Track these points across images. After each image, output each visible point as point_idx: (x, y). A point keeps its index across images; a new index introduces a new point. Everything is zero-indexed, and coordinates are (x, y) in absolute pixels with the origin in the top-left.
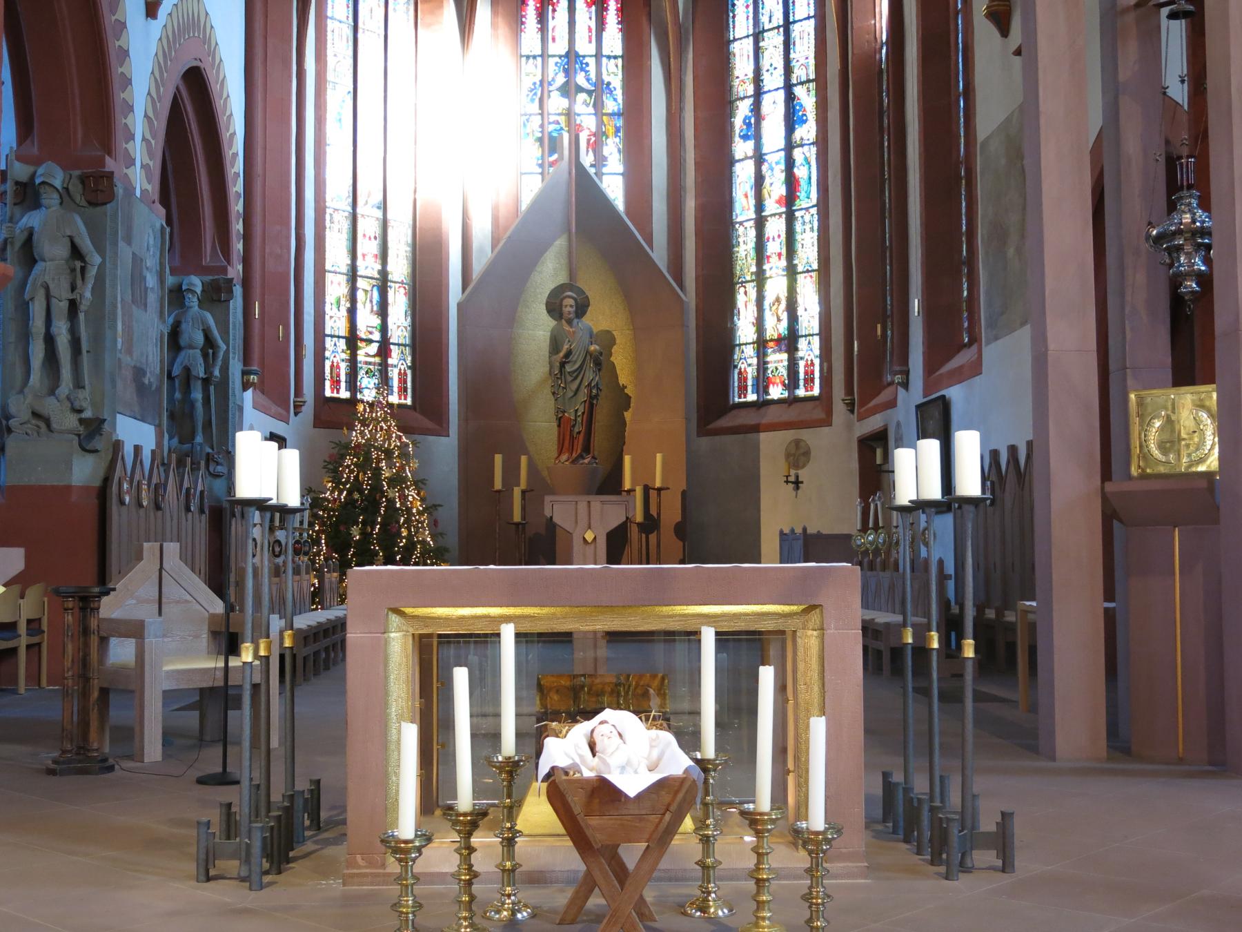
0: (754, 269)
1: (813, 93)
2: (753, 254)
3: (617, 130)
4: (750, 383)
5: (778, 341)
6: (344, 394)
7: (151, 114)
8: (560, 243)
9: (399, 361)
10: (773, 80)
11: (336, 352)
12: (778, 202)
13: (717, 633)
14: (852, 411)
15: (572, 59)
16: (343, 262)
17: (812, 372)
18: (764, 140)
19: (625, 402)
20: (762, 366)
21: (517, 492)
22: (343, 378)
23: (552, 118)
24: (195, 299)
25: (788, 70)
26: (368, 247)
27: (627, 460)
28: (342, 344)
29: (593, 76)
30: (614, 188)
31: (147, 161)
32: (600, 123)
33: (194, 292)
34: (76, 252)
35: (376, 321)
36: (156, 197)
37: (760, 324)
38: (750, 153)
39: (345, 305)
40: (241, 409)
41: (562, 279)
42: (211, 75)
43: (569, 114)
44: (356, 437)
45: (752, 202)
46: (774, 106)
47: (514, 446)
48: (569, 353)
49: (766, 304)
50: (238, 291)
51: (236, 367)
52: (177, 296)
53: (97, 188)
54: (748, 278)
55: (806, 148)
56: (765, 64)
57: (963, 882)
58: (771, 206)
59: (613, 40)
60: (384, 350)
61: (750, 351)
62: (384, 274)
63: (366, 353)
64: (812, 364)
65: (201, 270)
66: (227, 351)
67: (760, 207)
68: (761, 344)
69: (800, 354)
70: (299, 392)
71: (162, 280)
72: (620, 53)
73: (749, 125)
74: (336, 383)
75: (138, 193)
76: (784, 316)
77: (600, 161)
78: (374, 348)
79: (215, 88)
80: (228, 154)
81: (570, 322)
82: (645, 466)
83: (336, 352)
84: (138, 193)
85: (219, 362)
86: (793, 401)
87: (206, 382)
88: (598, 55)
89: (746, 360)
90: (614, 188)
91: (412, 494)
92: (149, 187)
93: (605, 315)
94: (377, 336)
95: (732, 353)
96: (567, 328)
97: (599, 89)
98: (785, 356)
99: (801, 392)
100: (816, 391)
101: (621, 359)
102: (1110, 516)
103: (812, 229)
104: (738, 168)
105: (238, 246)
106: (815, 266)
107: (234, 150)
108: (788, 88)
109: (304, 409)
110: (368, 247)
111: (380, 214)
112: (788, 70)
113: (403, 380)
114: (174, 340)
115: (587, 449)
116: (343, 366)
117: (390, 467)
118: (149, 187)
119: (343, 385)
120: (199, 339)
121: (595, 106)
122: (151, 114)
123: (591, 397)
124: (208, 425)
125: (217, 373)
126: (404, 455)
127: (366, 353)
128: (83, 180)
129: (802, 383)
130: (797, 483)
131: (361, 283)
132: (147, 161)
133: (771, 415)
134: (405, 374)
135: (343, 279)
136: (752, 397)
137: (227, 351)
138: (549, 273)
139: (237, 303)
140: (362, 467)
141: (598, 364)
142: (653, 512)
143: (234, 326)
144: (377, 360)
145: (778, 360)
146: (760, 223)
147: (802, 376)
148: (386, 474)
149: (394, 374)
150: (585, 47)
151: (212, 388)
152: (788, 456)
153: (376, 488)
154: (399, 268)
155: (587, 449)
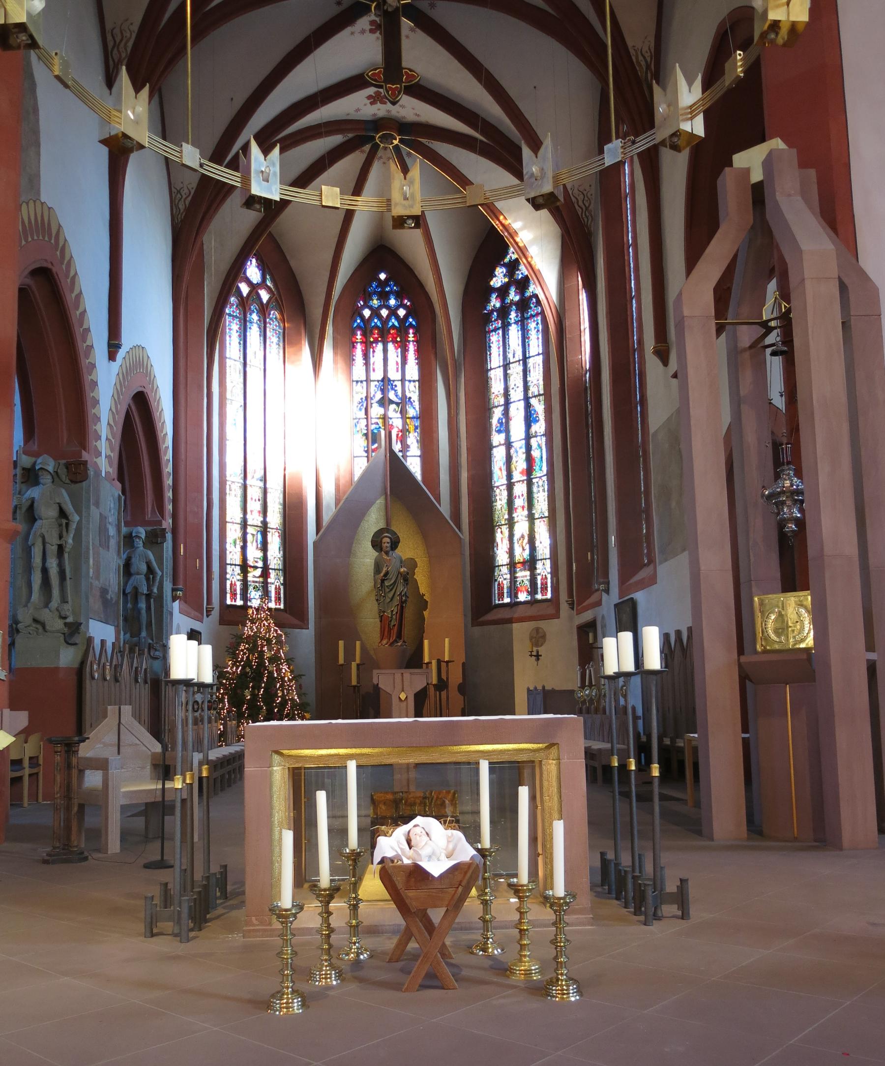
0: (506, 516)
1: (543, 402)
2: (505, 506)
3: (416, 428)
4: (505, 591)
5: (524, 563)
6: (239, 602)
7: (112, 423)
8: (380, 501)
9: (275, 580)
10: (517, 394)
11: (234, 575)
12: (522, 473)
13: (490, 763)
14: (573, 609)
15: (386, 382)
17: (546, 584)
18: (512, 433)
19: (424, 605)
20: (513, 579)
21: (354, 665)
22: (238, 592)
23: (374, 421)
24: (141, 542)
25: (526, 388)
26: (254, 506)
27: (426, 642)
28: (238, 570)
29: (400, 393)
30: (414, 465)
31: (109, 453)
32: (405, 424)
33: (140, 538)
34: (63, 514)
35: (260, 554)
36: (115, 476)
37: (511, 552)
38: (503, 442)
39: (239, 544)
40: (171, 614)
41: (382, 525)
42: (151, 397)
43: (385, 418)
44: (248, 630)
45: (504, 473)
46: (517, 412)
47: (351, 634)
48: (387, 574)
49: (515, 539)
50: (169, 536)
51: (168, 586)
52: (129, 540)
53: (76, 472)
54: (503, 523)
55: (539, 438)
56: (511, 384)
57: (656, 927)
58: (517, 476)
59: (413, 370)
60: (265, 573)
61: (505, 570)
62: (265, 524)
63: (254, 575)
64: (546, 578)
65: (144, 523)
66: (162, 576)
67: (509, 476)
69: (538, 571)
71: (119, 530)
72: (417, 378)
73: (501, 424)
74: (233, 596)
75: (103, 475)
76: (527, 547)
77: (405, 447)
78: (258, 572)
79: (153, 405)
80: (162, 447)
81: (387, 553)
82: (437, 647)
83: (234, 575)
84: (103, 475)
85: (157, 584)
86: (533, 602)
87: (148, 596)
88: (403, 380)
89: (503, 575)
90: (414, 465)
91: (285, 667)
92: (111, 470)
93: (410, 548)
94: (260, 564)
95: (494, 572)
96: (385, 557)
97: (404, 402)
98: (528, 573)
99: (539, 596)
100: (549, 596)
101: (421, 577)
102: (744, 678)
103: (544, 490)
104: (495, 451)
105: (169, 507)
106: (546, 514)
107: (166, 445)
108: (527, 399)
109: (213, 612)
110: (254, 506)
111: (262, 484)
112: (526, 388)
113: (278, 593)
114: (127, 569)
115: (399, 636)
116: (238, 584)
117: (270, 650)
118: (111, 470)
119: (238, 596)
120: (144, 568)
121: (401, 412)
122: (112, 423)
123: (402, 602)
124: (149, 624)
125: (155, 590)
126: (279, 642)
127: (254, 575)
128: (67, 466)
129: (539, 590)
130: (538, 656)
131: (250, 530)
132: (109, 453)
133: (519, 612)
134: (279, 588)
135: (238, 527)
136: (507, 600)
137: (162, 576)
138: (373, 521)
140: (251, 651)
141: (406, 580)
142: (444, 677)
143: (167, 559)
144: (261, 579)
145: (523, 575)
146: (510, 487)
147: (539, 586)
148: (267, 655)
149: (272, 589)
150: (394, 374)
151: (152, 600)
152: (531, 638)
153: (261, 664)
154: (275, 519)
155: (399, 636)
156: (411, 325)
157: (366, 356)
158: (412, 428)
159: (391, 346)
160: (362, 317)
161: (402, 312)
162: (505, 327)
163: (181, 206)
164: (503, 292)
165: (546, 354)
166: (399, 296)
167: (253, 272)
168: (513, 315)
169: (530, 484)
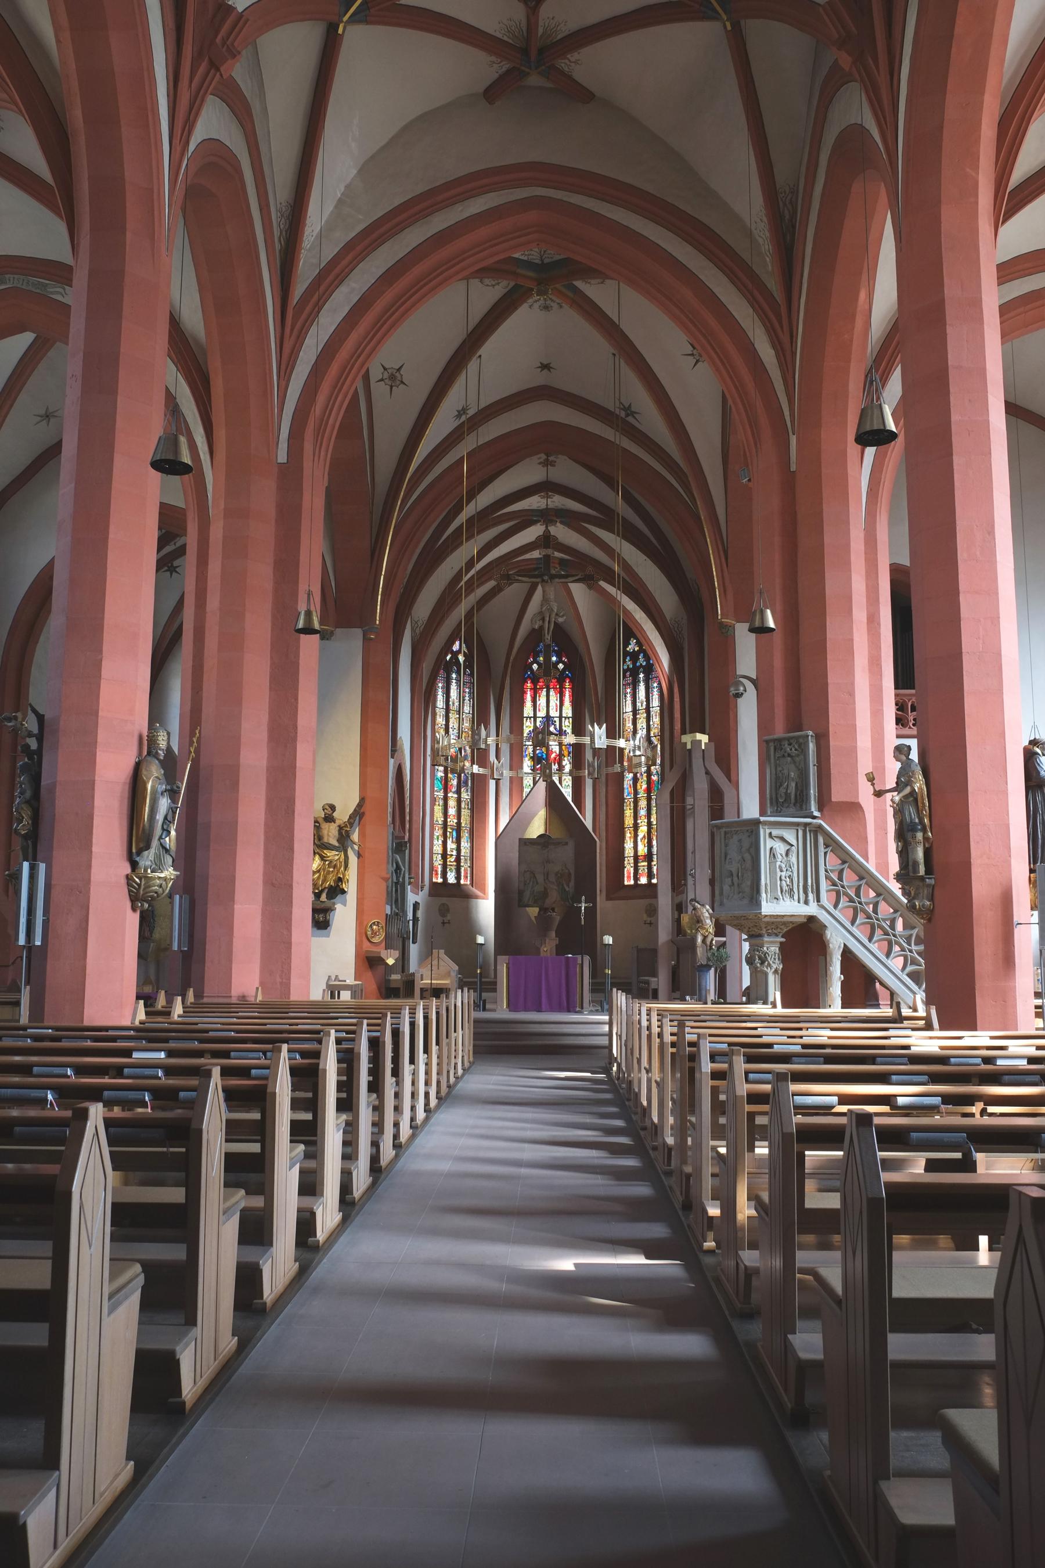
6: (440, 880)
15: (548, 718)
16: (441, 820)
26: (452, 811)
32: (561, 749)
35: (454, 846)
39: (441, 839)
58: (642, 794)
59: (568, 710)
60: (458, 859)
62: (459, 823)
63: (451, 860)
67: (636, 793)
68: (636, 857)
70: (423, 881)
83: (438, 862)
88: (561, 717)
94: (455, 853)
127: (451, 860)
139: (407, 852)
150: (554, 713)
156: (567, 676)
158: (566, 753)
159: (552, 692)
160: (532, 670)
161: (561, 666)
163: (418, 631)
164: (634, 656)
165: (662, 706)
168: (641, 676)
169: (649, 799)
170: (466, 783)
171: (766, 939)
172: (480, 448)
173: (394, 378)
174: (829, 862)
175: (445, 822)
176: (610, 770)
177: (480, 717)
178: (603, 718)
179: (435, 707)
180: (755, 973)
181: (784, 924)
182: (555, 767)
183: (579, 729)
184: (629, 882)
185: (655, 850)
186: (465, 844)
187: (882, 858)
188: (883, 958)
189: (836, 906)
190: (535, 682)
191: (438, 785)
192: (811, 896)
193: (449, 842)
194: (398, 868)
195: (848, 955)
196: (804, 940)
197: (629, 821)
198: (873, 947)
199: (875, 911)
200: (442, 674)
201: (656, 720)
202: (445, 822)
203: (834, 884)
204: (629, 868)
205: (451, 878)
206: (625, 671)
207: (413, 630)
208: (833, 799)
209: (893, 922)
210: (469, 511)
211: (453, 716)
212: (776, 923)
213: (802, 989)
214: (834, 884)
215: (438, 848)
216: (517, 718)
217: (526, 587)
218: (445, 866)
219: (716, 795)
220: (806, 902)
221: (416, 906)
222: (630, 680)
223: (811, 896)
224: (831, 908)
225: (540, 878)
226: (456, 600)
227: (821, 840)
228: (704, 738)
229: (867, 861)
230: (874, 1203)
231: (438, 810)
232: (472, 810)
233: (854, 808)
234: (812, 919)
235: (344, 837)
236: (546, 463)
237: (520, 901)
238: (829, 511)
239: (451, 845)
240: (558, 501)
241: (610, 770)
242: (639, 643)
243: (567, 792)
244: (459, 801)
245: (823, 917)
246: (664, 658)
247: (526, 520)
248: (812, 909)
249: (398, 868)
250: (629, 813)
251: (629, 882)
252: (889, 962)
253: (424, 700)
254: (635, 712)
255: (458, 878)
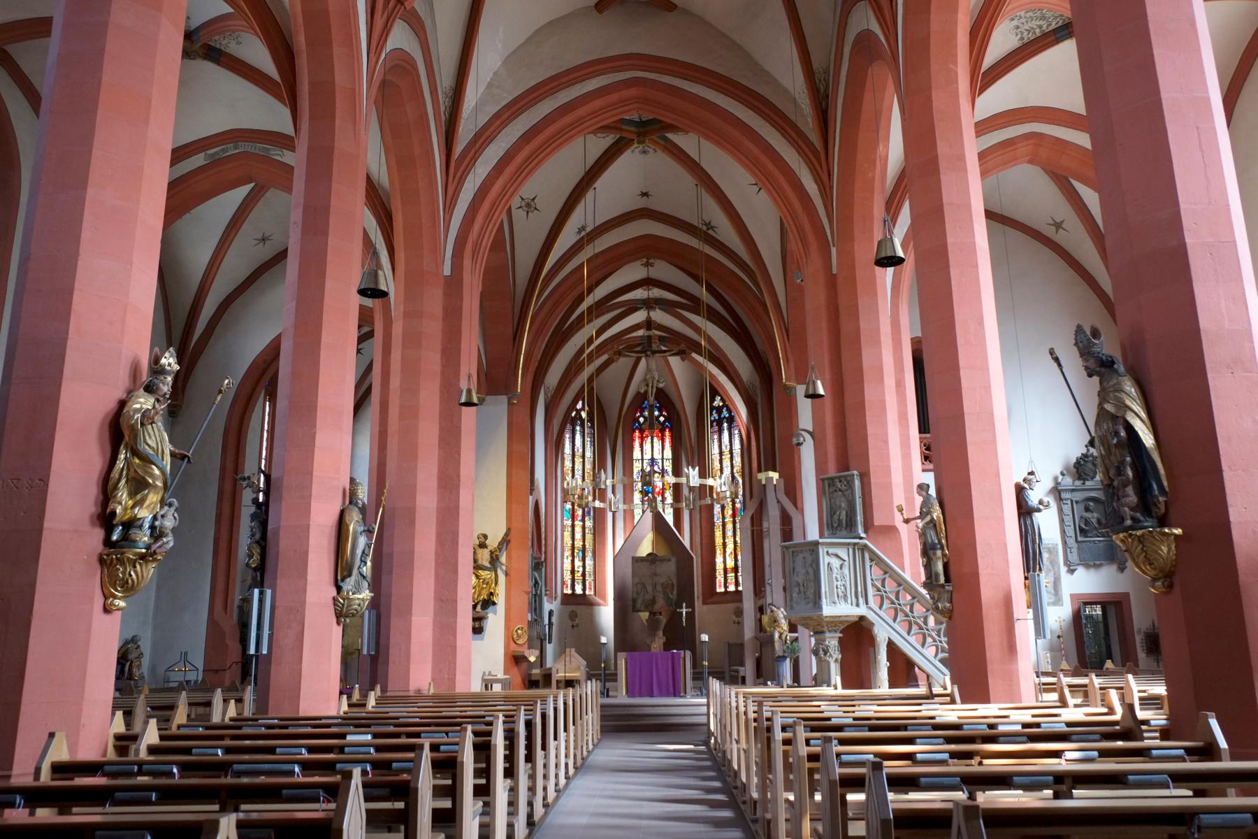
6: (569, 592)
15: (653, 460)
26: (578, 536)
35: (581, 564)
37: (725, 562)
59: (668, 453)
60: (584, 575)
62: (584, 546)
63: (578, 575)
67: (724, 518)
68: (725, 570)
83: (568, 577)
127: (578, 575)
150: (657, 456)
157: (641, 446)
159: (655, 439)
161: (662, 419)
162: (720, 432)
164: (719, 410)
165: (742, 449)
166: (660, 411)
167: (579, 406)
169: (734, 523)
170: (589, 513)
171: (828, 635)
172: (596, 256)
173: (529, 206)
174: (874, 573)
175: (573, 545)
176: (703, 502)
177: (599, 463)
178: (696, 460)
179: (563, 453)
180: (819, 661)
181: (841, 622)
182: (659, 498)
183: (677, 472)
184: (720, 589)
185: (740, 563)
186: (589, 562)
187: (912, 570)
188: (919, 647)
189: (881, 607)
190: (642, 432)
191: (567, 515)
192: (861, 600)
193: (576, 560)
194: (536, 582)
195: (891, 645)
196: (857, 635)
197: (719, 540)
198: (912, 639)
199: (912, 611)
200: (569, 427)
201: (738, 460)
202: (573, 545)
203: (879, 590)
204: (720, 578)
205: (579, 590)
206: (712, 422)
207: (545, 394)
208: (876, 523)
209: (926, 619)
210: (589, 301)
211: (578, 461)
212: (834, 622)
213: (857, 675)
214: (879, 590)
215: (567, 566)
216: (628, 461)
217: (631, 361)
218: (573, 580)
219: (786, 520)
220: (858, 605)
221: (551, 613)
222: (716, 428)
223: (861, 600)
224: (876, 608)
225: (650, 588)
226: (580, 368)
227: (867, 556)
228: (775, 476)
229: (903, 570)
230: (885, 822)
231: (567, 535)
232: (594, 534)
233: (891, 530)
234: (862, 618)
235: (494, 560)
236: (647, 265)
237: (634, 607)
238: (862, 302)
239: (578, 563)
240: (656, 293)
241: (703, 502)
242: (722, 399)
243: (669, 517)
244: (584, 528)
245: (871, 616)
246: (742, 411)
247: (632, 308)
248: (862, 611)
249: (536, 582)
250: (718, 534)
251: (720, 589)
252: (924, 651)
253: (555, 446)
254: (721, 453)
255: (584, 589)
